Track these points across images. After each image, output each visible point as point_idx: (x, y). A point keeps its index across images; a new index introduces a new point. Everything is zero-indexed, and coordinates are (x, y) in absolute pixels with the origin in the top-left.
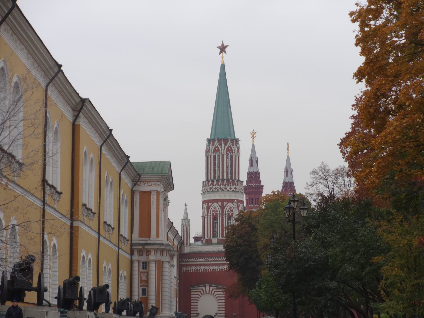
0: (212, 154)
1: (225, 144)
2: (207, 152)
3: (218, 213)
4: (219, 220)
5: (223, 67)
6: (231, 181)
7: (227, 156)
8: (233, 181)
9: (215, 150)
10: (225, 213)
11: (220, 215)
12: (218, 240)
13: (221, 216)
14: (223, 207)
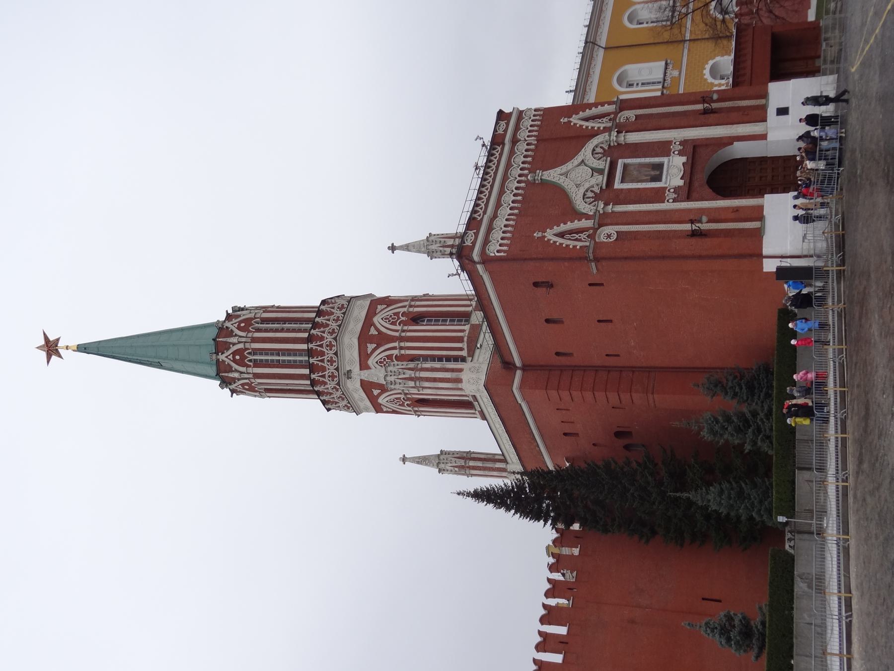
0: (250, 370)
1: (231, 334)
2: (250, 389)
3: (395, 352)
4: (414, 349)
5: (84, 348)
6: (317, 319)
7: (258, 330)
9: (241, 363)
10: (397, 331)
11: (401, 348)
12: (469, 356)
13: (402, 344)
14: (382, 339)
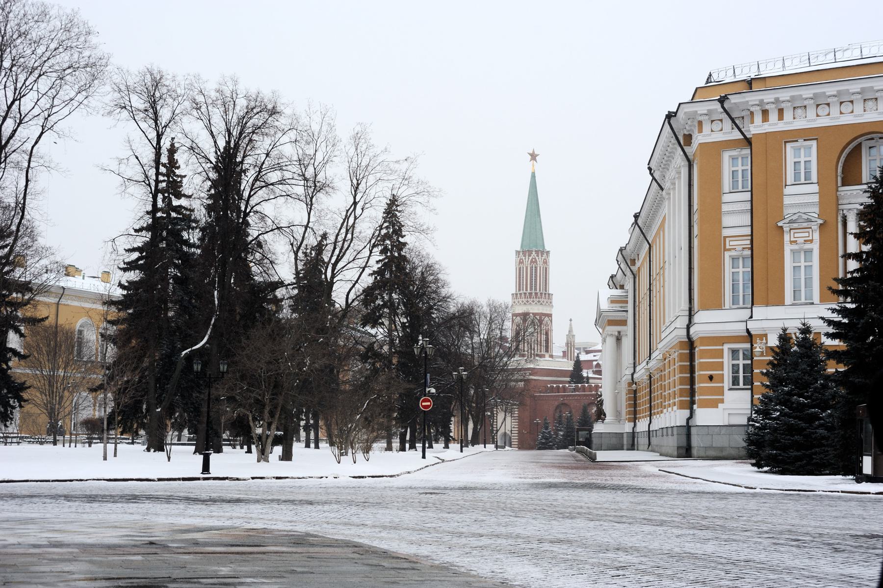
5: (533, 176)
8: (536, 294)
